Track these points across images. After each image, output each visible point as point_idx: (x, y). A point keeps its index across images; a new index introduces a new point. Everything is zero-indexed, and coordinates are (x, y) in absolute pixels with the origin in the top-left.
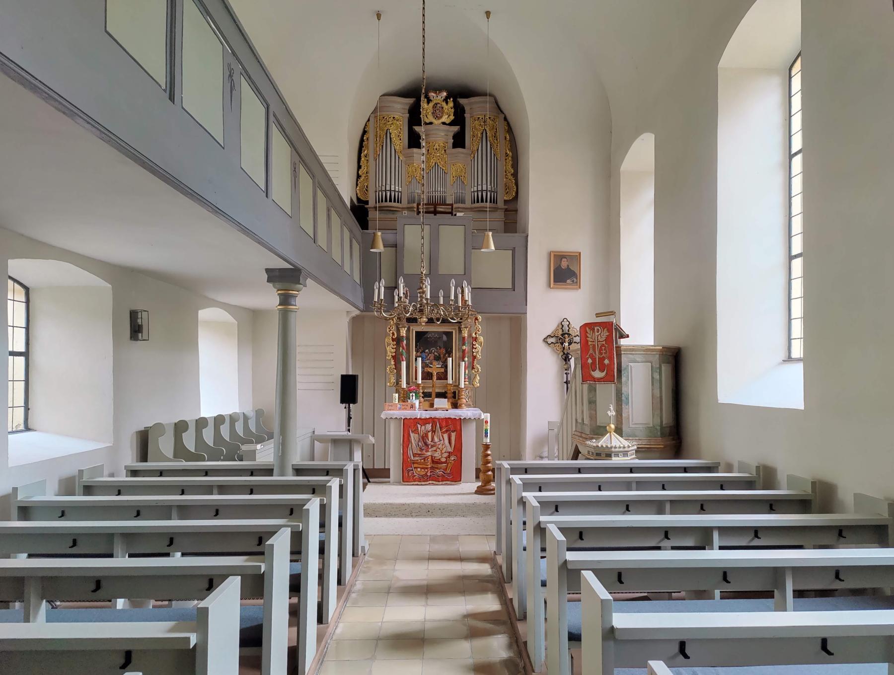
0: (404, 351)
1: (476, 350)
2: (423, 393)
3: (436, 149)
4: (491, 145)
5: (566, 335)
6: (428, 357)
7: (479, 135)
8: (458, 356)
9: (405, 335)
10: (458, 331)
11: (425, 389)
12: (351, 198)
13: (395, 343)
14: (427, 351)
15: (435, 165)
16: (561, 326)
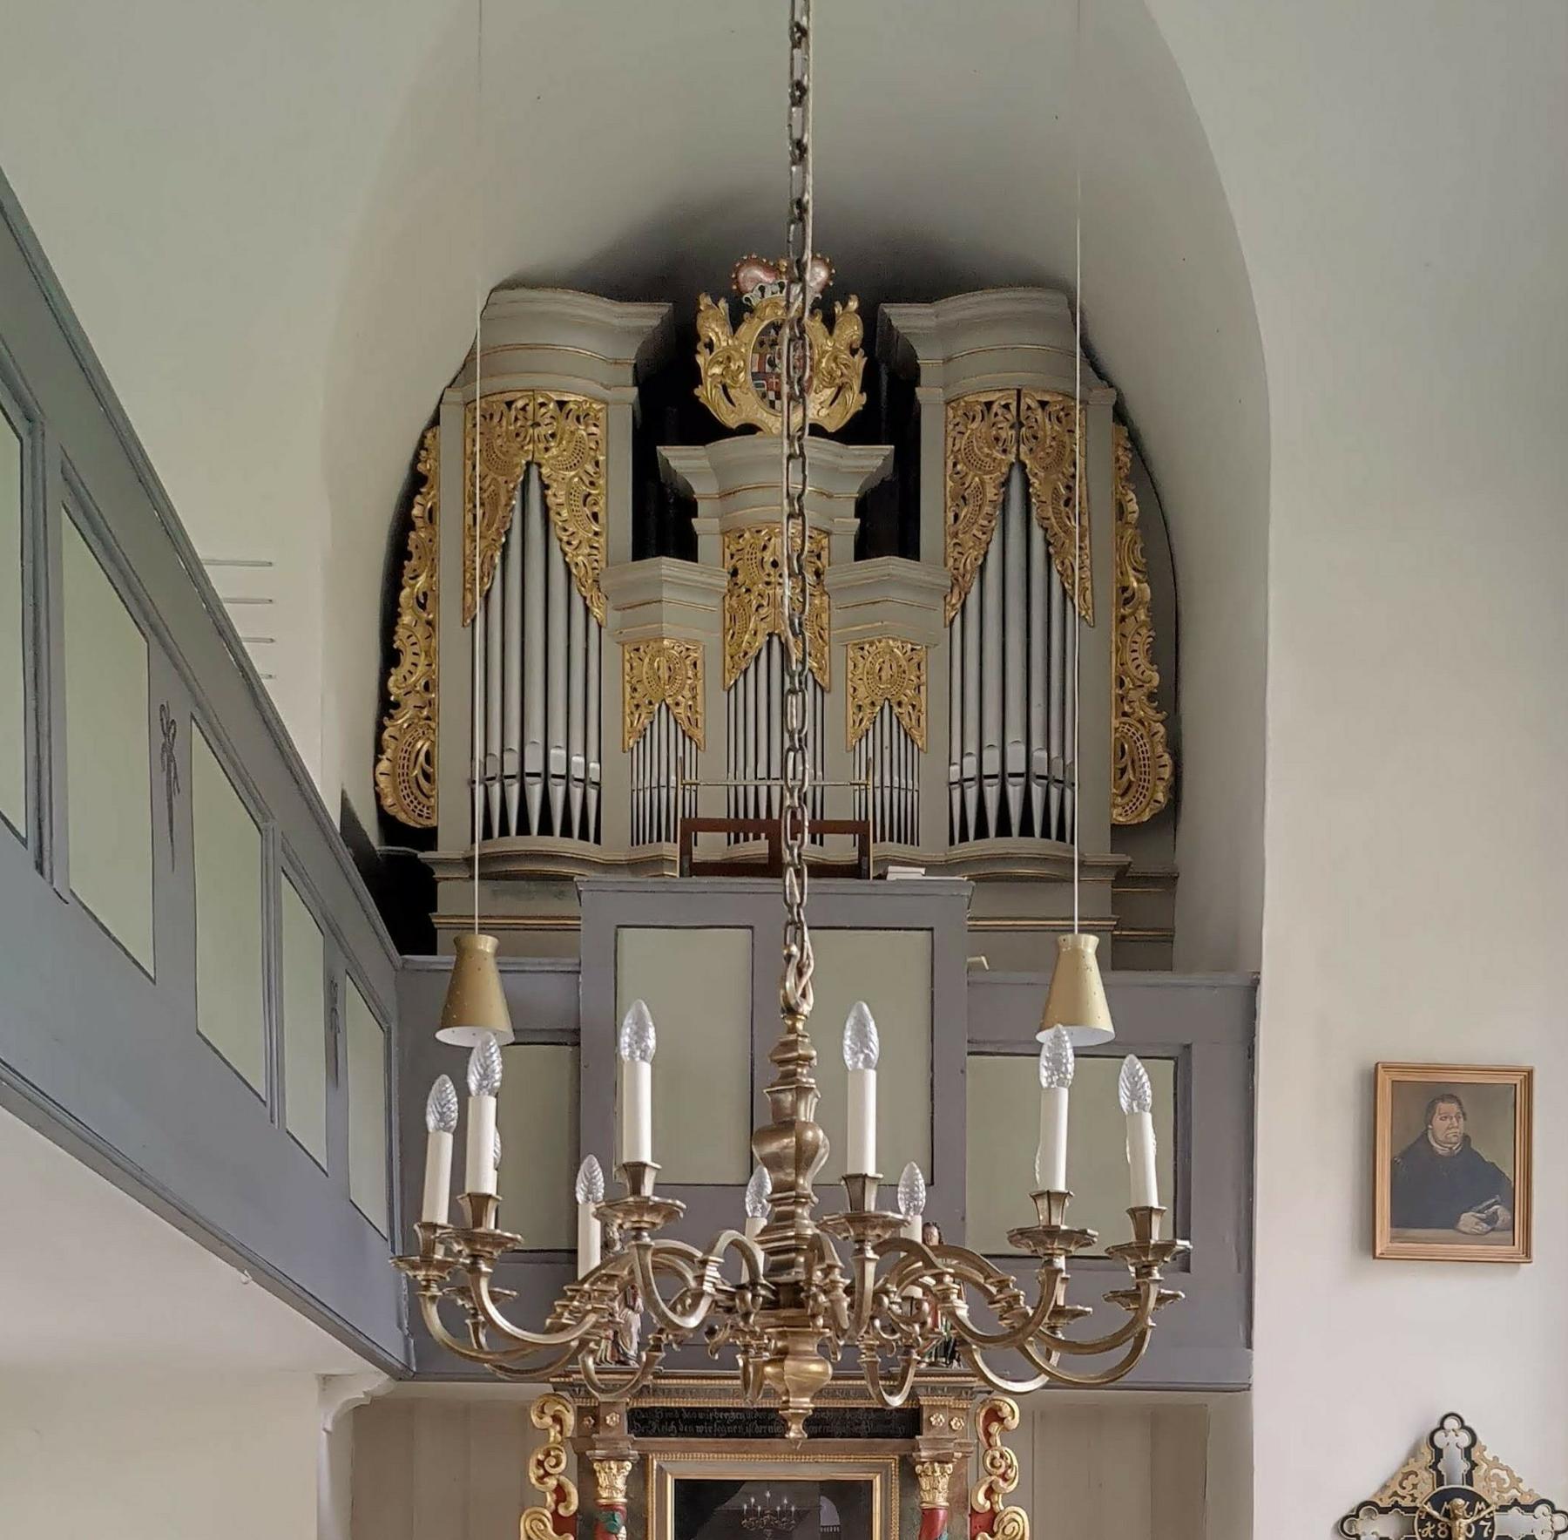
3: (775, 564)
4: (1048, 544)
5: (1460, 1502)
7: (991, 493)
9: (620, 1499)
10: (896, 1482)
12: (343, 792)
15: (769, 643)
16: (1427, 1456)
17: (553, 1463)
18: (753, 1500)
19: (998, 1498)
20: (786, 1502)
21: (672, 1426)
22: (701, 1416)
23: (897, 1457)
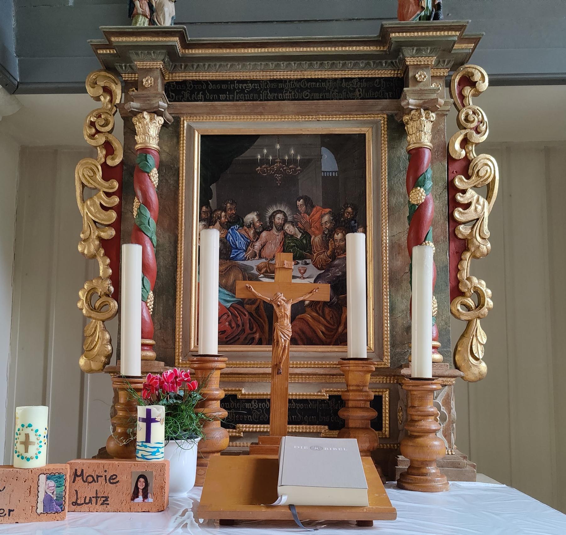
0: (148, 214)
1: (470, 214)
2: (227, 402)
6: (258, 245)
8: (386, 239)
9: (153, 144)
11: (242, 384)
13: (116, 185)
14: (251, 217)
17: (103, 123)
18: (265, 151)
19: (472, 148)
20: (292, 152)
21: (200, 95)
22: (224, 87)
23: (385, 116)
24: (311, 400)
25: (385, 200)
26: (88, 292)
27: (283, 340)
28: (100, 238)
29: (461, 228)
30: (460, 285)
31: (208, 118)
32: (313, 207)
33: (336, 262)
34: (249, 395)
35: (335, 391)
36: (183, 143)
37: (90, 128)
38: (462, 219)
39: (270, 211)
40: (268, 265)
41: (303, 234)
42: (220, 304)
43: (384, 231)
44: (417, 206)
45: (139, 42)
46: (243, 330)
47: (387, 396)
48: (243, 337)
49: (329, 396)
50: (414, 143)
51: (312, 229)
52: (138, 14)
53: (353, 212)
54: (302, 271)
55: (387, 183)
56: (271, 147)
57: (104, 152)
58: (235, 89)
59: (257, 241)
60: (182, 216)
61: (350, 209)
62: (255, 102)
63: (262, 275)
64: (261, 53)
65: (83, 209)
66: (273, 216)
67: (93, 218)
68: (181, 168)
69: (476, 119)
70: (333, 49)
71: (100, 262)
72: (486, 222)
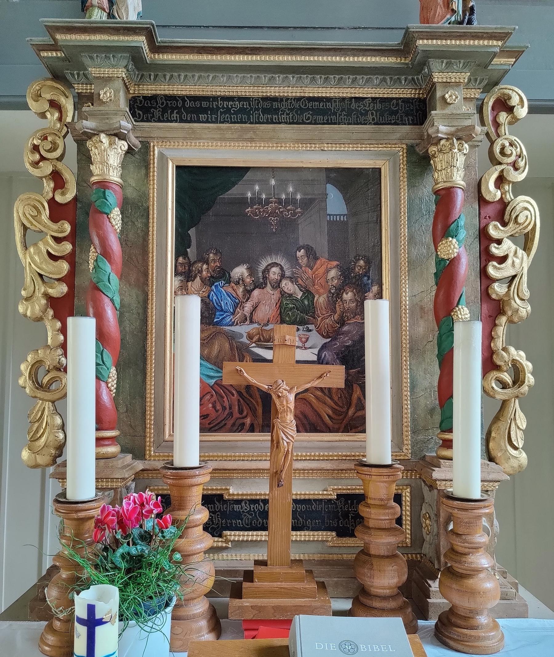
0: (107, 267)
1: (507, 270)
6: (248, 307)
8: (406, 301)
9: (114, 176)
11: (229, 480)
13: (67, 227)
20: (291, 189)
21: (175, 115)
22: (204, 104)
24: (315, 500)
25: (405, 251)
26: (32, 366)
27: (285, 444)
28: (47, 296)
29: (495, 287)
30: (494, 356)
31: (185, 144)
32: (316, 258)
33: (346, 328)
34: (238, 495)
35: (344, 489)
36: (153, 176)
37: (32, 153)
38: (497, 275)
39: (264, 264)
40: (261, 332)
41: (304, 293)
42: (201, 381)
43: (404, 289)
44: (448, 262)
45: (93, 41)
46: (231, 414)
47: (408, 494)
48: (230, 422)
49: (337, 495)
50: (445, 182)
51: (316, 287)
52: (92, 6)
53: (365, 266)
54: (304, 340)
55: (406, 230)
56: (264, 183)
57: (52, 185)
58: (218, 108)
59: (247, 301)
60: (153, 269)
61: (362, 263)
62: (244, 125)
63: (254, 345)
64: (252, 61)
65: (25, 259)
66: (266, 270)
67: (38, 270)
68: (151, 208)
69: (514, 153)
70: (343, 59)
71: (48, 327)
72: (525, 278)
